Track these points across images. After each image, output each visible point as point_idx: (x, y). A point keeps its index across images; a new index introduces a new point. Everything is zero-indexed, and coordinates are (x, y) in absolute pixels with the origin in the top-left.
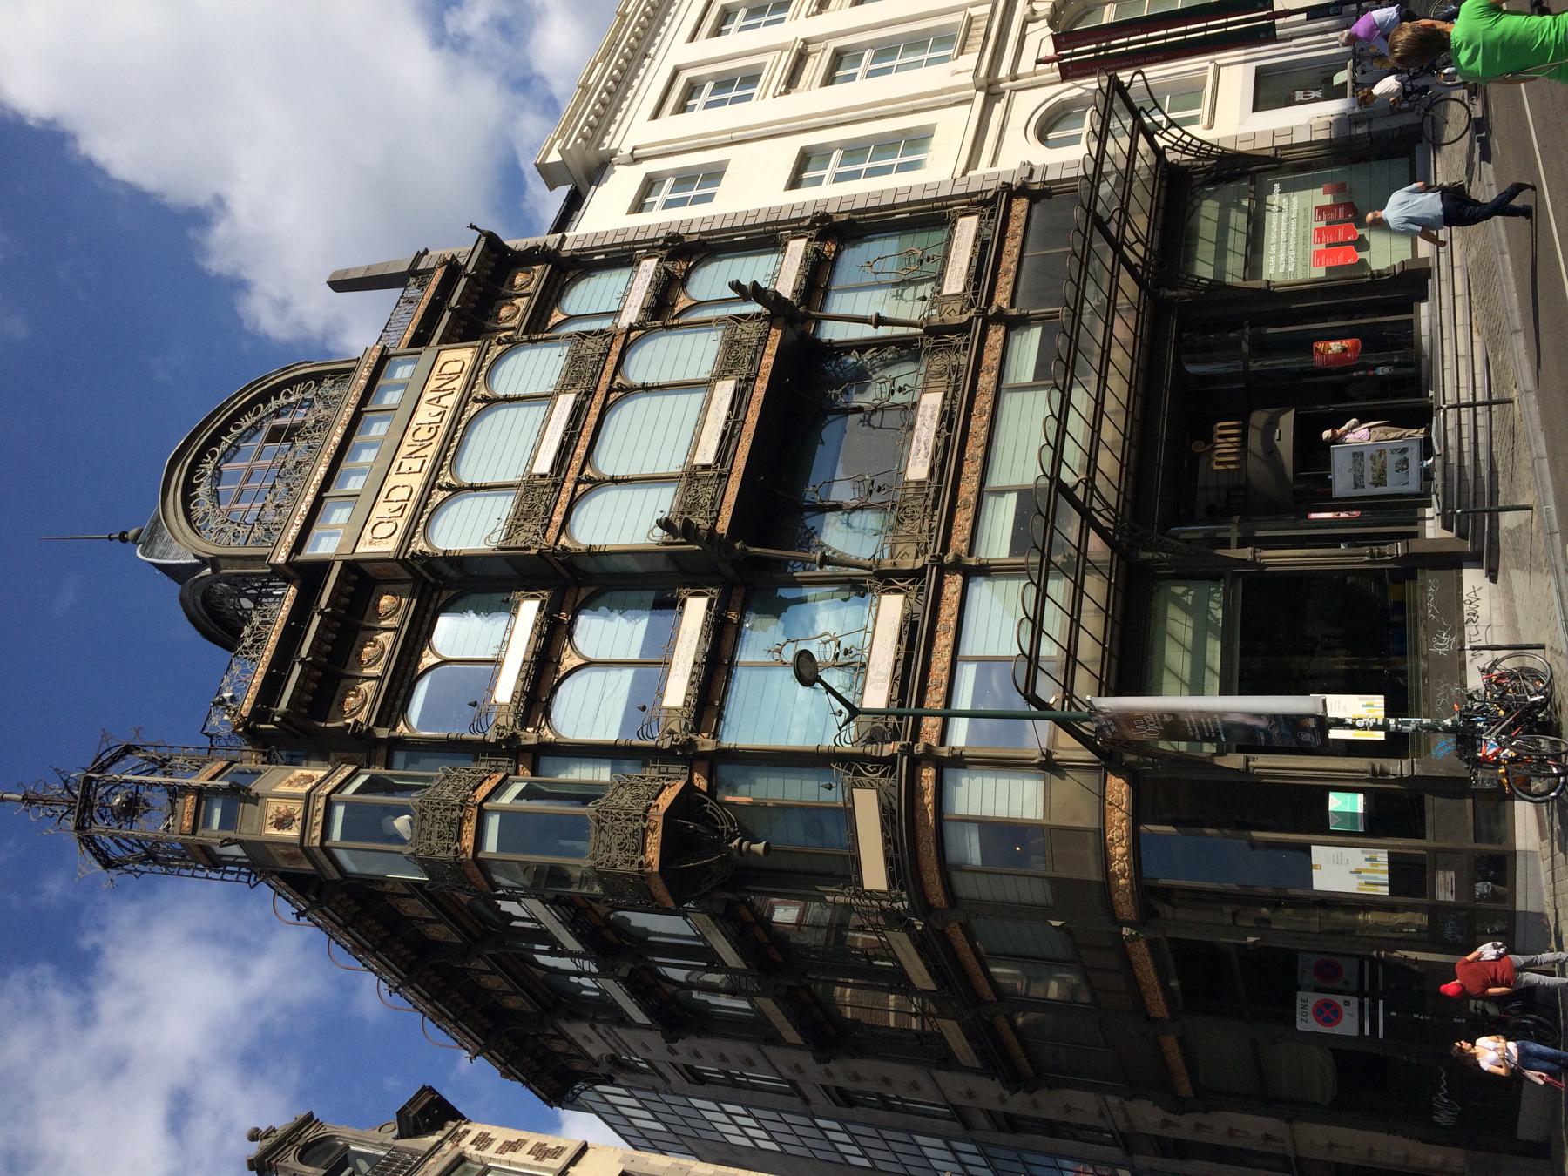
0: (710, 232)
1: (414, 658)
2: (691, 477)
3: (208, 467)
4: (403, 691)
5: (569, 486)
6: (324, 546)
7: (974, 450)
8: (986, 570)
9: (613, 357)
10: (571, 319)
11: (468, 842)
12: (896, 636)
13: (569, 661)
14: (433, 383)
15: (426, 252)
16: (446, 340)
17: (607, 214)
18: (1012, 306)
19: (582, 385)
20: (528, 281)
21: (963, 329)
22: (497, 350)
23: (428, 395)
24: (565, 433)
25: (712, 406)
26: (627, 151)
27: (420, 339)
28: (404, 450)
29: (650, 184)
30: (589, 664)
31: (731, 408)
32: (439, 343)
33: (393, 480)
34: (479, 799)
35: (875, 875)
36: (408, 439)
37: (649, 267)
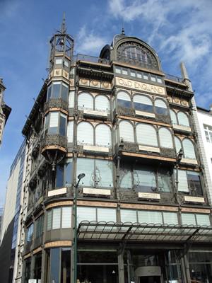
2: (136, 145)
3: (135, 45)
6: (117, 71)
7: (146, 207)
8: (118, 212)
10: (176, 114)
11: (53, 109)
13: (95, 124)
16: (167, 88)
17: (201, 119)
18: (183, 212)
20: (185, 104)
21: (176, 202)
22: (165, 99)
28: (140, 83)
30: (94, 128)
35: (51, 193)
37: (190, 130)
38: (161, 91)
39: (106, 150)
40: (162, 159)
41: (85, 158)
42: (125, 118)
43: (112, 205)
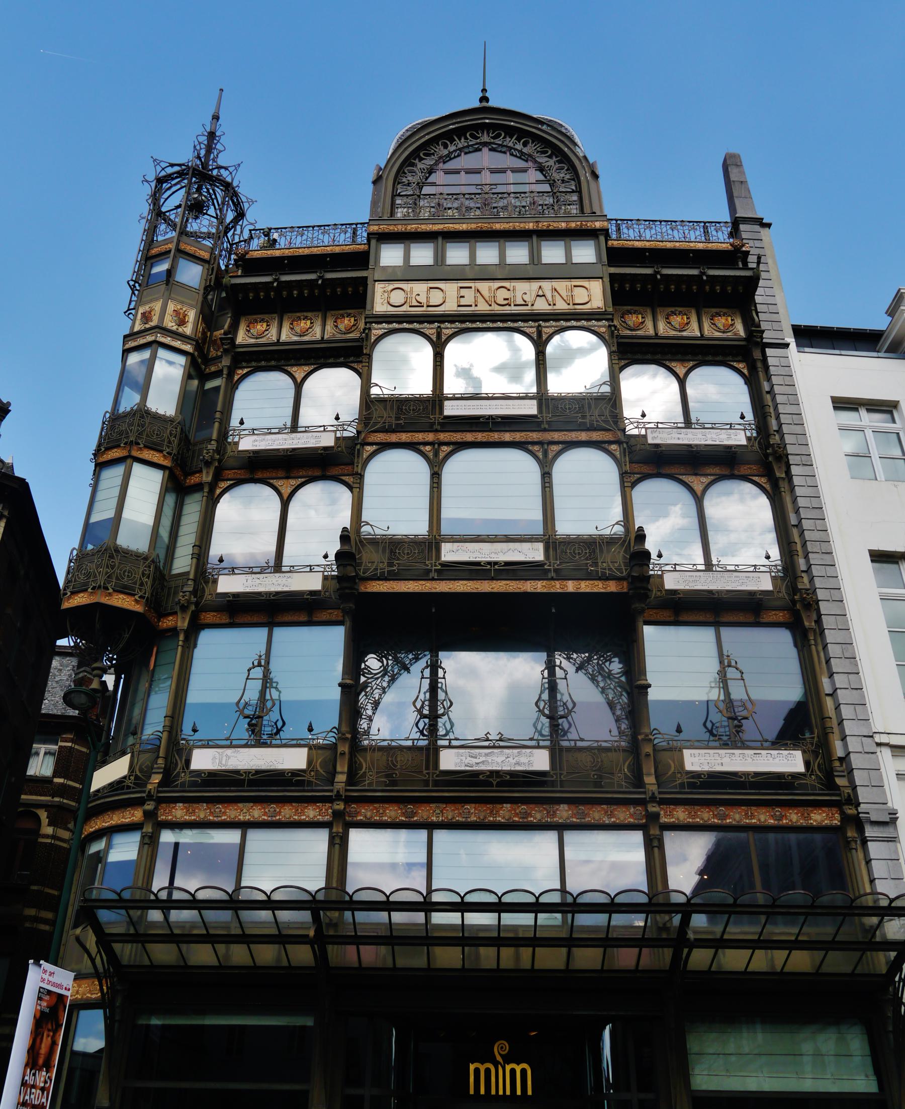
0: (792, 489)
1: (302, 361)
5: (430, 437)
7: (473, 813)
9: (583, 436)
12: (264, 767)
13: (286, 486)
14: (562, 286)
15: (769, 225)
17: (814, 379)
23: (547, 285)
25: (511, 545)
27: (616, 255)
31: (507, 564)
32: (611, 275)
33: (451, 288)
34: (135, 453)
38: (580, 296)
39: (313, 583)
40: (557, 587)
41: (231, 625)
42: (394, 438)
43: (311, 813)
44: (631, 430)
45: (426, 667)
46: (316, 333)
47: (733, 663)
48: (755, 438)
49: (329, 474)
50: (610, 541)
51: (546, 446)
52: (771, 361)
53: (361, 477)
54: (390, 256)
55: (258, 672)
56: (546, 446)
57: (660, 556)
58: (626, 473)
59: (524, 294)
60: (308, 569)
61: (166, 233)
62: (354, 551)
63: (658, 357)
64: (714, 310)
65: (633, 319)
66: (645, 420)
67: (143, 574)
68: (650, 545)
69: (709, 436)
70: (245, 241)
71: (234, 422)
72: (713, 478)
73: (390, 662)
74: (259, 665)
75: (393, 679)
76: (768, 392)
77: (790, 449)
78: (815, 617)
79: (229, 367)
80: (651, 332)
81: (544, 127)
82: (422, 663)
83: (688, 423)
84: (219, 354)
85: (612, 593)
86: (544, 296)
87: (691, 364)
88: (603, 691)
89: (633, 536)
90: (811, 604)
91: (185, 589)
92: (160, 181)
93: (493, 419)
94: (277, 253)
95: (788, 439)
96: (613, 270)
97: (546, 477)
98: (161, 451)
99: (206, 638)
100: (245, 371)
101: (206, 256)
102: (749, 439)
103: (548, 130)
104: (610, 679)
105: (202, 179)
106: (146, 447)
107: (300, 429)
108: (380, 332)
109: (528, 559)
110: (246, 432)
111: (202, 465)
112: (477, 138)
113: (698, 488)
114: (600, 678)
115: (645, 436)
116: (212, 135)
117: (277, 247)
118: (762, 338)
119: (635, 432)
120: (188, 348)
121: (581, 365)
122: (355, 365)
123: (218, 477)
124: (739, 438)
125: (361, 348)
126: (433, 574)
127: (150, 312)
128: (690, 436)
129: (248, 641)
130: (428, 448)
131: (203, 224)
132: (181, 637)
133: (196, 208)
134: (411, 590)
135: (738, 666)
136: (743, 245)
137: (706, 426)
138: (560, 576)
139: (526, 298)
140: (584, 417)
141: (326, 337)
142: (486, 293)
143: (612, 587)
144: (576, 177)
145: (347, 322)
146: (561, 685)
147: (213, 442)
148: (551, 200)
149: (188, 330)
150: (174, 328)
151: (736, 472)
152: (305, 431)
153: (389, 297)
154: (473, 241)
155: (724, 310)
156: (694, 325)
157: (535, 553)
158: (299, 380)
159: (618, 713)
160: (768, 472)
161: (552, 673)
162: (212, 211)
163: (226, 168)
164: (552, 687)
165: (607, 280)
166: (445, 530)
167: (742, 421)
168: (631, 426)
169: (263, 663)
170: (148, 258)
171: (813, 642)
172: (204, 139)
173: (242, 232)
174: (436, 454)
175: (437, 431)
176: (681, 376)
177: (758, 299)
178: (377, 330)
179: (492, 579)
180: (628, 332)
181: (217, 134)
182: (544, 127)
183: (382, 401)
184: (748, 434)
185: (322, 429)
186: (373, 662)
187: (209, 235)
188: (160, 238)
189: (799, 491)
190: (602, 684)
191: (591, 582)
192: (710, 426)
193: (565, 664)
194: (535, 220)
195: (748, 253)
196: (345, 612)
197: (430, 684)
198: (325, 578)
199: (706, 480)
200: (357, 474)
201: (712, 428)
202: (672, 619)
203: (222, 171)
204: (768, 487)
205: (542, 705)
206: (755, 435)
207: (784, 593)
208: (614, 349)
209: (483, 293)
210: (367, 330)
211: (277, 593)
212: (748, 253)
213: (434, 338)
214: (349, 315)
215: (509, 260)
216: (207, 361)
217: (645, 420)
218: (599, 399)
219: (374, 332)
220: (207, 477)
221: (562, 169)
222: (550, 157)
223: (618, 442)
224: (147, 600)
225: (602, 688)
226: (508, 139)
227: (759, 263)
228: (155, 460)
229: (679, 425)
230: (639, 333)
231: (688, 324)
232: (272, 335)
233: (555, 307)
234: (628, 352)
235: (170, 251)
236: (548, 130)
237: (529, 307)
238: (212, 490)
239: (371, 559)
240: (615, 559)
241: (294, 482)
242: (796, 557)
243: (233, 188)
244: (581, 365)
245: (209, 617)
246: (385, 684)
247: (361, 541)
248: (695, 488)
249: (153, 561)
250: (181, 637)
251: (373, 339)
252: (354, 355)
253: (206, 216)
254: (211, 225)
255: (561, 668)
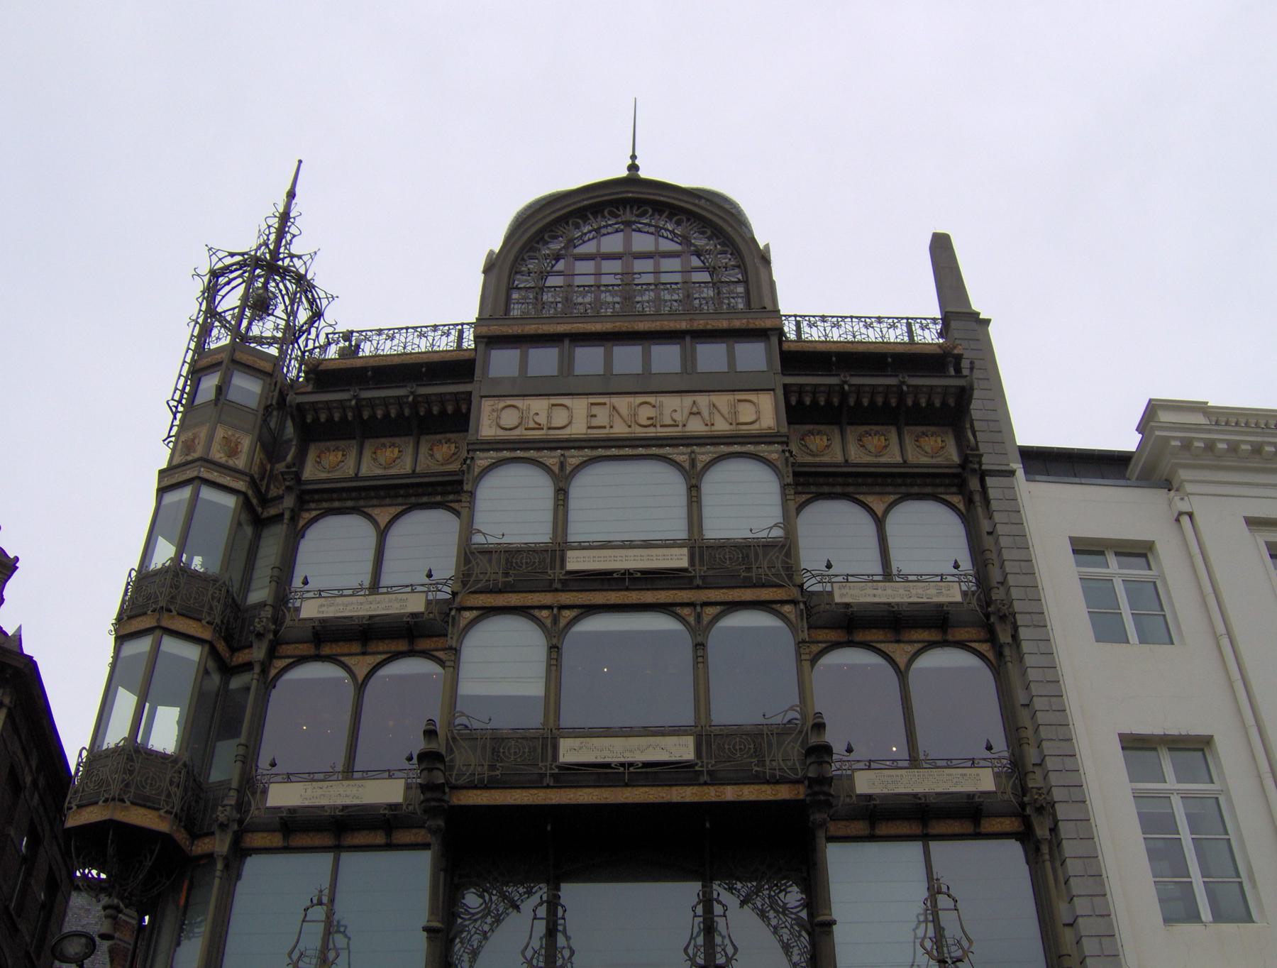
0: (1021, 658)
1: (388, 501)
4: (350, 504)
5: (547, 598)
9: (748, 595)
13: (362, 665)
14: (722, 401)
15: (987, 322)
19: (701, 570)
20: (933, 450)
23: (703, 401)
24: (627, 572)
25: (652, 739)
26: (1184, 507)
28: (622, 403)
29: (1139, 551)
31: (647, 765)
32: (785, 386)
33: (579, 406)
36: (640, 399)
40: (711, 794)
41: (287, 849)
42: (500, 600)
44: (812, 585)
45: (541, 904)
46: (405, 466)
47: (944, 889)
48: (973, 593)
49: (417, 648)
50: (784, 731)
51: (699, 609)
52: (992, 493)
53: (456, 651)
54: (504, 362)
55: (319, 913)
56: (699, 609)
57: (849, 750)
58: (804, 642)
59: (674, 411)
60: (386, 775)
61: (218, 339)
62: (444, 752)
63: (850, 489)
64: (920, 429)
65: (817, 442)
66: (831, 572)
67: (171, 782)
68: (835, 738)
69: (914, 592)
70: (320, 347)
71: (297, 582)
72: (920, 646)
73: (494, 898)
74: (320, 903)
75: (498, 920)
76: (990, 533)
77: (1018, 606)
78: (1048, 823)
79: (292, 510)
80: (839, 458)
81: (702, 202)
82: (535, 899)
83: (887, 575)
84: (281, 492)
85: (784, 802)
86: (699, 413)
87: (892, 498)
88: (775, 930)
89: (810, 723)
90: (1046, 808)
91: (225, 802)
92: (215, 274)
93: (630, 574)
94: (358, 363)
95: (1015, 593)
96: (789, 380)
97: (700, 646)
98: (200, 620)
99: (253, 865)
100: (314, 513)
101: (268, 367)
102: (964, 594)
103: (707, 206)
104: (784, 914)
105: (269, 270)
106: (179, 614)
107: (381, 590)
108: (485, 463)
109: (673, 759)
110: (311, 595)
111: (252, 637)
112: (616, 216)
113: (901, 660)
114: (772, 914)
115: (831, 594)
116: (285, 217)
117: (361, 354)
118: (980, 463)
119: (818, 588)
120: (240, 485)
121: (744, 503)
122: (455, 505)
123: (272, 653)
124: (953, 594)
125: (461, 483)
126: (548, 780)
127: (193, 441)
128: (889, 592)
129: (309, 870)
130: (545, 613)
131: (266, 328)
132: (220, 866)
133: (260, 305)
134: (518, 802)
135: (951, 892)
136: (955, 348)
137: (911, 578)
138: (715, 779)
139: (677, 417)
140: (749, 569)
141: (418, 470)
142: (624, 411)
143: (783, 793)
144: (742, 266)
145: (443, 451)
146: (721, 924)
147: (268, 608)
148: (711, 293)
149: (240, 462)
150: (223, 460)
151: (950, 638)
152: (388, 593)
153: (499, 417)
154: (609, 344)
155: (933, 429)
156: (895, 449)
157: (682, 749)
158: (382, 526)
159: (796, 958)
160: (992, 638)
161: (708, 910)
162: (279, 312)
163: (300, 257)
164: (709, 929)
165: (780, 392)
166: (568, 719)
167: (955, 571)
168: (813, 581)
169: (325, 900)
170: (196, 372)
171: (1047, 857)
172: (275, 222)
173: (317, 336)
174: (555, 621)
175: (556, 590)
176: (880, 514)
177: (975, 414)
178: (483, 460)
179: (627, 785)
180: (809, 459)
181: (292, 215)
182: (702, 202)
183: (487, 552)
184: (964, 588)
185: (409, 589)
186: (472, 900)
187: (274, 340)
188: (213, 346)
189: (1029, 660)
190: (774, 922)
191: (757, 787)
192: (914, 578)
193: (726, 897)
194: (688, 317)
195: (959, 358)
196: (433, 832)
197: (548, 928)
198: (408, 787)
199: (911, 649)
200: (451, 648)
201: (918, 581)
202: (867, 832)
203: (295, 260)
204: (990, 655)
205: (690, 951)
206: (974, 588)
207: (1009, 796)
208: (790, 480)
209: (621, 410)
210: (468, 461)
211: (345, 807)
212: (959, 358)
213: (556, 469)
214: (448, 441)
215: (656, 368)
216: (265, 501)
217: (831, 572)
218: (768, 546)
219: (480, 463)
220: (258, 653)
221: (725, 253)
222: (709, 239)
223: (794, 602)
224: (176, 815)
225: (775, 928)
226: (657, 217)
227: (972, 369)
228: (192, 632)
229: (876, 578)
230: (826, 459)
231: (886, 447)
232: (349, 469)
233: (714, 428)
234: (808, 484)
235: (220, 364)
236: (707, 206)
237: (679, 429)
238: (264, 671)
239: (466, 760)
240: (788, 756)
241: (372, 660)
242: (1025, 746)
243: (308, 281)
244: (744, 503)
245: (258, 840)
246: (486, 928)
247: (454, 739)
248: (898, 660)
249: (185, 765)
250: (220, 866)
251: (477, 470)
252: (448, 492)
253: (271, 318)
254: (277, 328)
255: (719, 902)
